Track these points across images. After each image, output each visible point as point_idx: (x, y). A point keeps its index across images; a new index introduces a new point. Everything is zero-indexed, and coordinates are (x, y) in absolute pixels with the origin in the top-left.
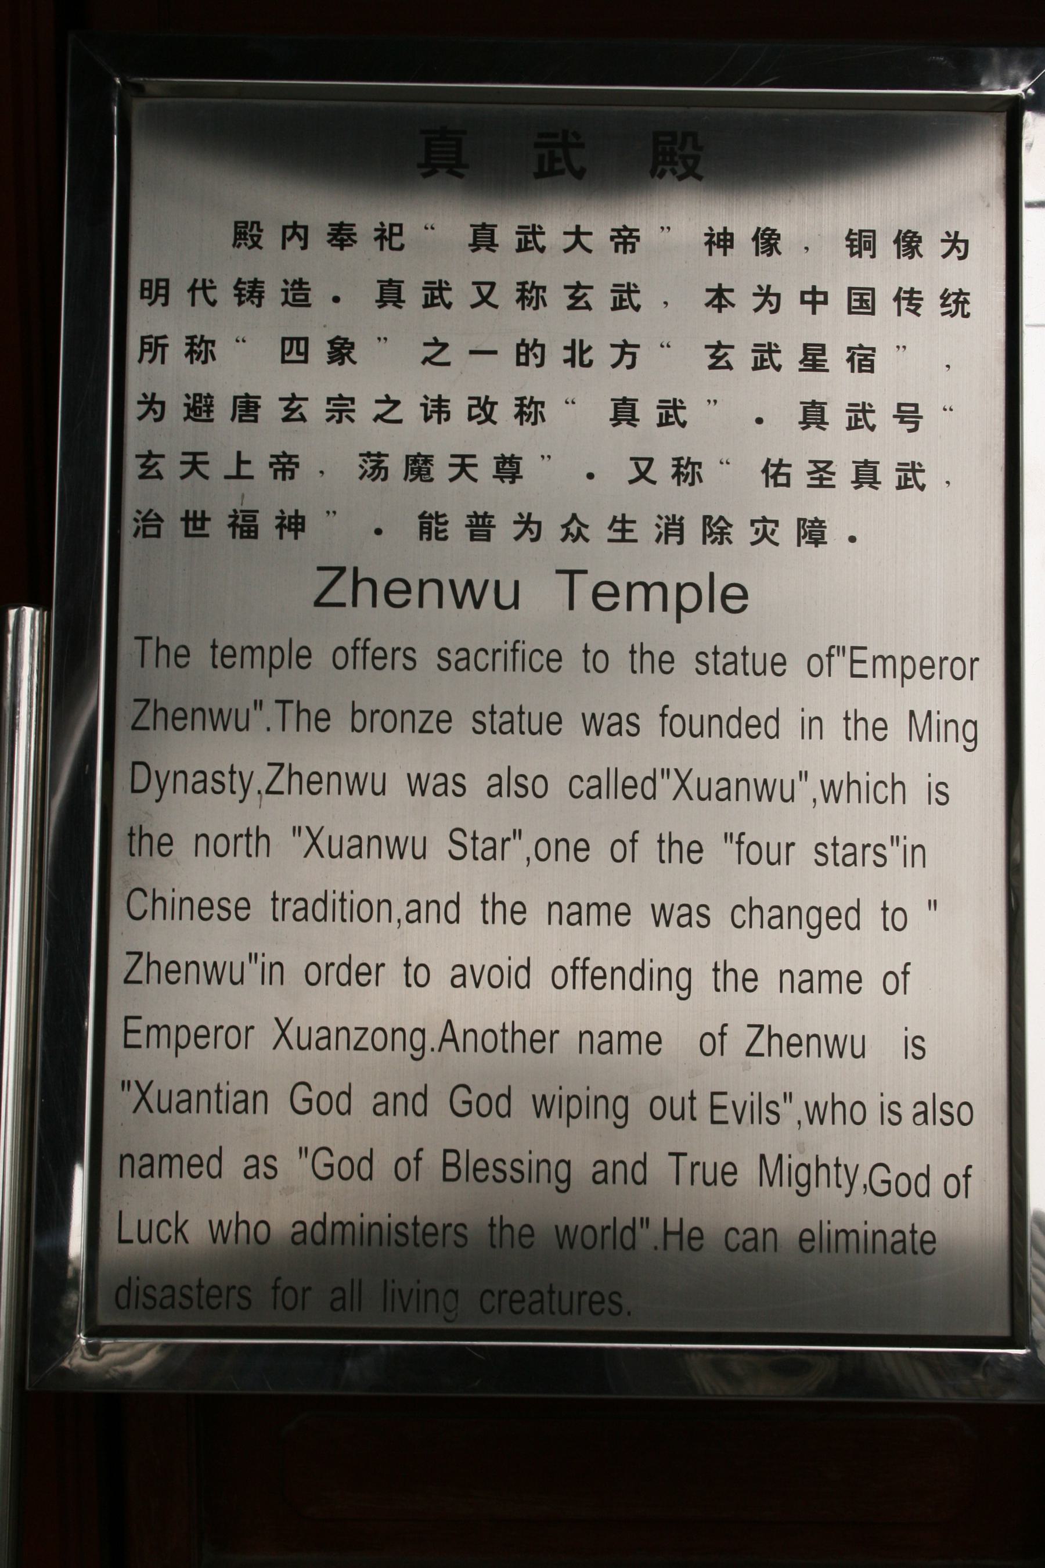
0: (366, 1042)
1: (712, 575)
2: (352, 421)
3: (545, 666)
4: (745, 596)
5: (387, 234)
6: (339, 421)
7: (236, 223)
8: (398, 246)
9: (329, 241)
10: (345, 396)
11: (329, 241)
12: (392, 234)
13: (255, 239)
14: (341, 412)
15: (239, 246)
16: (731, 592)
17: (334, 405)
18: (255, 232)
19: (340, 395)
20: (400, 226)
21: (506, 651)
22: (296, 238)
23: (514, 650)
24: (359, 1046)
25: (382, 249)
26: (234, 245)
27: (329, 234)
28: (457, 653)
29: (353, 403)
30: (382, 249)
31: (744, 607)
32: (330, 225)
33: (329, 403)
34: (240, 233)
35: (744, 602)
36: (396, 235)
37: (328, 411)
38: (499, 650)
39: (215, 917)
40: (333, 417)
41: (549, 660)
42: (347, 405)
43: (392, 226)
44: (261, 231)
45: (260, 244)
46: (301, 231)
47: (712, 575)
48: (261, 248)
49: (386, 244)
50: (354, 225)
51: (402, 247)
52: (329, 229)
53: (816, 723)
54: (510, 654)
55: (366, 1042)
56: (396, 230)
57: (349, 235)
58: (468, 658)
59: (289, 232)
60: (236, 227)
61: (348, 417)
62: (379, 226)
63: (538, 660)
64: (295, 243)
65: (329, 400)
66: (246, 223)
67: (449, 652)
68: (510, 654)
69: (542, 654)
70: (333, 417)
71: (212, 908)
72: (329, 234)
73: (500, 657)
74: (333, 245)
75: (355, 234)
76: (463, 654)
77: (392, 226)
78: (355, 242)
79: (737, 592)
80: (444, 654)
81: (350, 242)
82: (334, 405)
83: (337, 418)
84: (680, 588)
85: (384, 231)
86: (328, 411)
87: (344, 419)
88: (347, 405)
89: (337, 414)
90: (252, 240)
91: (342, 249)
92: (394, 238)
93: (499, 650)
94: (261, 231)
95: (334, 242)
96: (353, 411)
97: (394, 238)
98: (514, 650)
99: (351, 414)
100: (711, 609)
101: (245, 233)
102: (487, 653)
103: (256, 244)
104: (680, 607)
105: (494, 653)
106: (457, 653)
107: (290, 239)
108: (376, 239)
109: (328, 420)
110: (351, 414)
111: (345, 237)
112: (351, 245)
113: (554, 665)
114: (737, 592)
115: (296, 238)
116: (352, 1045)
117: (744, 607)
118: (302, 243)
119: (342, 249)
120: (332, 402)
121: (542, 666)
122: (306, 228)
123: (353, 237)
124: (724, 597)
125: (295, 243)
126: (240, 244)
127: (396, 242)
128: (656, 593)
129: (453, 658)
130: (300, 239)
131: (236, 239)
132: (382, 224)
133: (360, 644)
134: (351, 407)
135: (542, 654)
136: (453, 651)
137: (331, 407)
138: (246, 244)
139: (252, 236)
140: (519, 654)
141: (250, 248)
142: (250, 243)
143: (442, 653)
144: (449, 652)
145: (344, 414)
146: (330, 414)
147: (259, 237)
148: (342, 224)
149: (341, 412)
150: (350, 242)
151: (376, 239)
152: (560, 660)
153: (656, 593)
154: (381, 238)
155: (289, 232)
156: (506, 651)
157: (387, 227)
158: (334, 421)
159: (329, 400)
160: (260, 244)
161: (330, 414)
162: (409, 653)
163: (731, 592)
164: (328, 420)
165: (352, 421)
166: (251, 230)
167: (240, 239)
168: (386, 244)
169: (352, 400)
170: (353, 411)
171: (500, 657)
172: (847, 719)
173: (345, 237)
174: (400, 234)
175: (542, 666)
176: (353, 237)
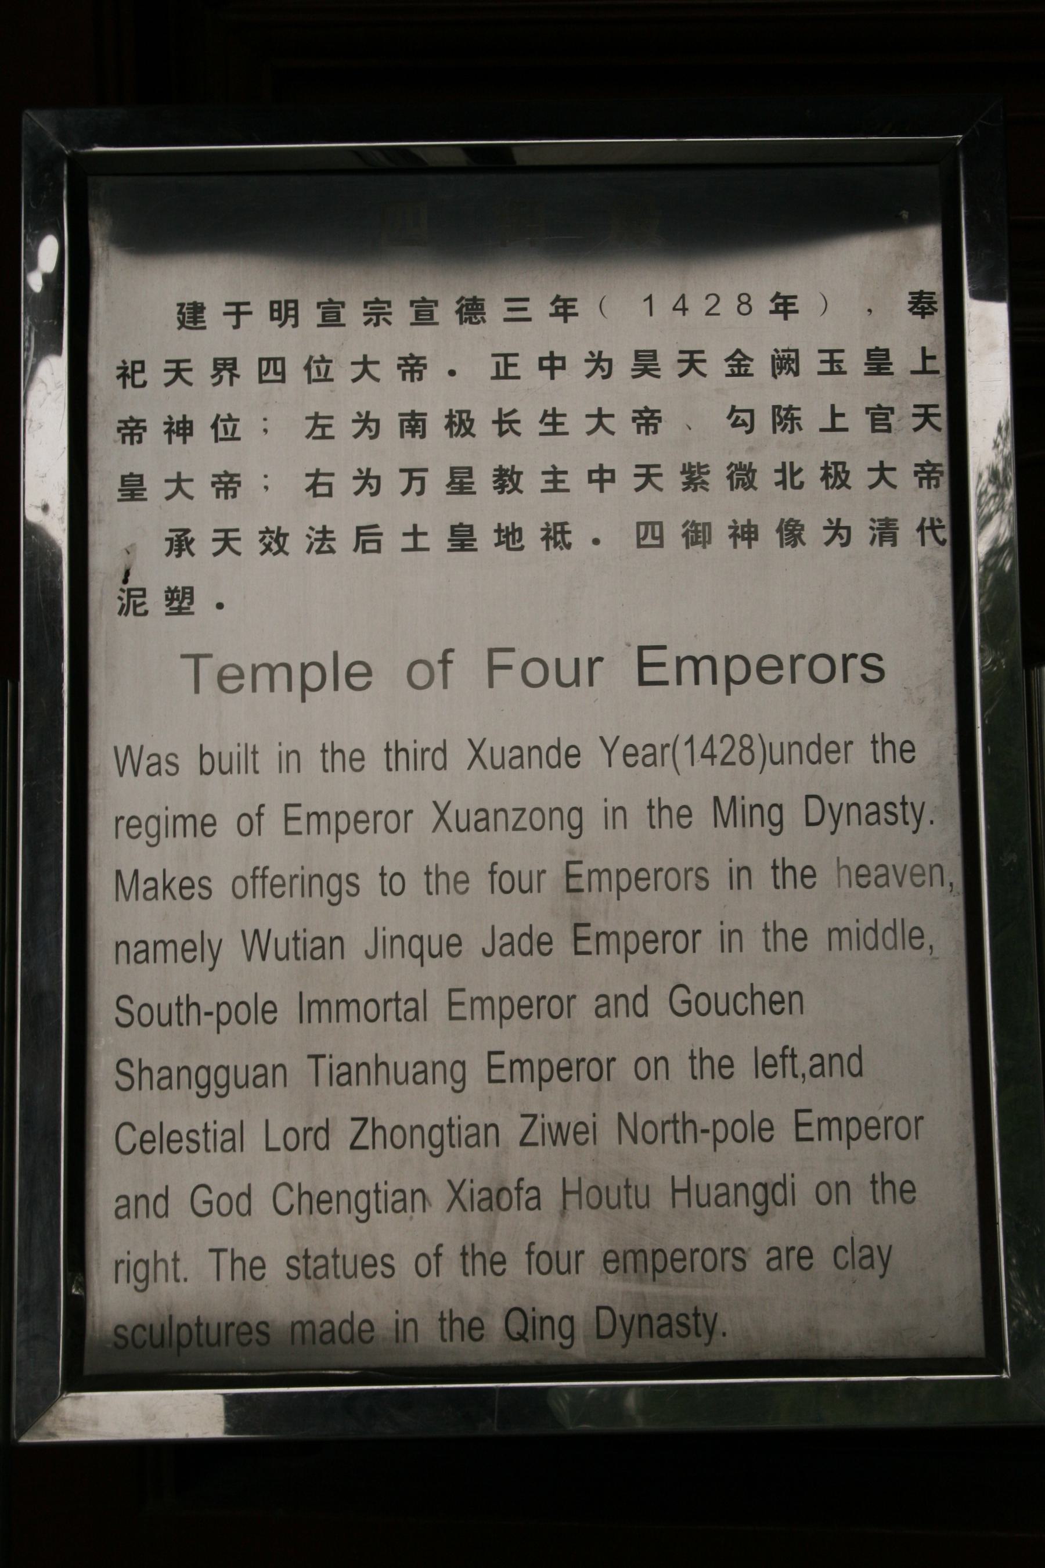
2: (389, 323)
5: (129, 372)
10: (381, 299)
12: (134, 372)
20: (142, 363)
25: (124, 386)
56: (138, 367)
61: (384, 319)
87: (382, 322)
88: (384, 308)
96: (390, 314)
99: (388, 317)
110: (388, 317)
134: (387, 310)
145: (381, 317)
149: (378, 315)
165: (389, 323)
170: (390, 314)
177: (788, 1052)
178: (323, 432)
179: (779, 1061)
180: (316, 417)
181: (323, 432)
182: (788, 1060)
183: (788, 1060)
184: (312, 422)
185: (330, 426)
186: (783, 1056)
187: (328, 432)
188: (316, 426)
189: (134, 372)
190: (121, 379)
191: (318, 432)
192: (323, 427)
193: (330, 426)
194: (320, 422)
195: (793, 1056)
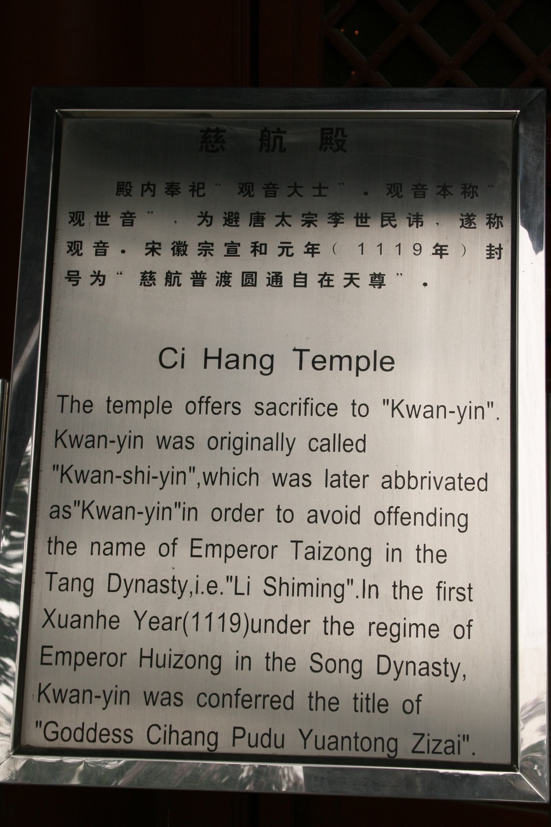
0: (182, 663)
1: (375, 352)
2: (212, 255)
4: (393, 363)
5: (196, 188)
6: (205, 255)
7: (118, 183)
9: (166, 192)
10: (208, 242)
11: (166, 192)
12: (199, 188)
14: (206, 250)
16: (386, 360)
17: (202, 247)
18: (128, 187)
19: (206, 242)
24: (177, 665)
25: (193, 196)
26: (117, 195)
27: (166, 188)
29: (212, 246)
30: (193, 196)
31: (392, 368)
32: (166, 183)
33: (199, 246)
34: (120, 188)
35: (392, 365)
36: (201, 188)
37: (199, 250)
40: (202, 253)
42: (209, 247)
43: (199, 184)
44: (132, 187)
45: (131, 194)
46: (152, 187)
47: (375, 352)
48: (131, 196)
49: (195, 193)
50: (179, 183)
51: (204, 195)
52: (166, 186)
55: (182, 663)
57: (176, 189)
59: (145, 187)
60: (118, 185)
61: (209, 253)
62: (192, 184)
64: (149, 193)
65: (200, 244)
66: (123, 183)
70: (202, 253)
72: (166, 188)
74: (168, 194)
75: (180, 188)
77: (199, 184)
78: (180, 192)
79: (389, 360)
81: (177, 192)
82: (202, 247)
83: (204, 254)
84: (358, 358)
85: (194, 186)
86: (199, 250)
87: (208, 254)
89: (204, 252)
90: (127, 192)
91: (172, 196)
92: (200, 190)
94: (132, 187)
95: (169, 192)
96: (213, 250)
97: (200, 190)
99: (211, 252)
100: (375, 370)
101: (123, 188)
103: (128, 194)
104: (358, 368)
107: (146, 191)
108: (190, 191)
109: (199, 255)
110: (211, 252)
111: (174, 190)
112: (177, 194)
114: (389, 360)
116: (172, 665)
117: (392, 368)
118: (152, 193)
119: (172, 196)
120: (202, 245)
122: (154, 185)
123: (179, 190)
124: (382, 363)
125: (149, 193)
126: (120, 194)
127: (201, 192)
128: (346, 361)
130: (151, 191)
131: (118, 192)
132: (193, 183)
134: (211, 248)
137: (200, 248)
139: (126, 190)
141: (125, 196)
142: (125, 193)
145: (208, 252)
146: (200, 252)
147: (130, 190)
148: (173, 183)
149: (206, 250)
150: (177, 192)
151: (190, 191)
153: (346, 361)
154: (193, 190)
157: (196, 185)
158: (202, 255)
159: (200, 244)
160: (131, 194)
161: (200, 252)
163: (386, 360)
164: (199, 255)
165: (212, 255)
166: (126, 187)
167: (120, 191)
168: (195, 193)
169: (212, 244)
170: (213, 250)
173: (174, 190)
174: (203, 188)
176: (179, 190)
189: (199, 188)
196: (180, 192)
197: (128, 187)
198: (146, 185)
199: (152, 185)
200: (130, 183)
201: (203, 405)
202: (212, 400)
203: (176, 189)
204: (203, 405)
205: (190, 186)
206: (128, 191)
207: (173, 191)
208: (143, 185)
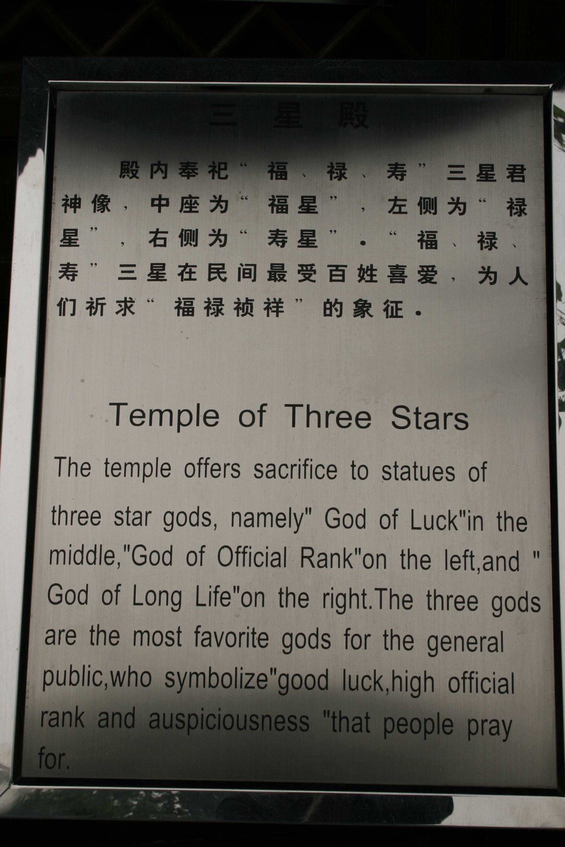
3: (326, 475)
5: (217, 169)
8: (224, 176)
9: (180, 174)
13: (134, 172)
15: (124, 177)
18: (134, 168)
21: (300, 465)
22: (160, 172)
23: (305, 465)
25: (213, 178)
26: (120, 176)
28: (267, 467)
30: (213, 178)
34: (125, 169)
38: (295, 465)
39: (286, 728)
41: (328, 471)
44: (138, 167)
45: (137, 175)
46: (163, 168)
48: (138, 178)
49: (216, 175)
51: (226, 177)
53: (478, 520)
54: (302, 468)
58: (274, 470)
59: (155, 168)
60: (122, 165)
63: (321, 472)
64: (159, 175)
66: (129, 162)
67: (262, 466)
68: (302, 468)
69: (324, 468)
71: (284, 722)
73: (296, 469)
74: (183, 176)
75: (197, 169)
76: (271, 468)
78: (197, 174)
80: (259, 467)
81: (193, 174)
85: (215, 167)
90: (132, 173)
91: (188, 178)
93: (295, 465)
94: (138, 167)
95: (183, 174)
97: (222, 172)
98: (305, 465)
101: (128, 169)
102: (287, 467)
103: (134, 176)
105: (292, 466)
106: (267, 467)
107: (156, 172)
108: (209, 172)
111: (191, 171)
112: (194, 176)
113: (332, 475)
115: (160, 172)
118: (163, 175)
119: (188, 178)
121: (324, 475)
122: (166, 165)
123: (196, 171)
125: (159, 175)
129: (265, 470)
130: (162, 172)
131: (122, 173)
133: (203, 461)
135: (324, 468)
136: (265, 466)
138: (128, 176)
139: (132, 171)
140: (308, 468)
141: (131, 178)
143: (257, 467)
144: (262, 466)
147: (137, 171)
150: (193, 174)
152: (336, 471)
155: (155, 168)
156: (300, 465)
160: (137, 175)
162: (235, 467)
166: (132, 167)
168: (216, 175)
171: (296, 469)
172: (499, 517)
173: (191, 171)
175: (324, 475)
176: (196, 171)
177: (468, 554)
178: (400, 209)
179: (462, 559)
180: (396, 200)
181: (400, 209)
182: (468, 559)
183: (468, 559)
184: (392, 203)
185: (405, 205)
186: (465, 556)
187: (403, 209)
188: (395, 205)
189: (220, 169)
190: (211, 173)
191: (397, 209)
192: (400, 206)
193: (405, 205)
194: (398, 203)
195: (472, 556)
196: (197, 174)
197: (134, 168)
198: (155, 165)
199: (163, 165)
200: (136, 163)
201: (203, 467)
202: (210, 462)
203: (193, 170)
204: (203, 467)
205: (210, 166)
206: (134, 172)
207: (188, 173)
208: (152, 166)
